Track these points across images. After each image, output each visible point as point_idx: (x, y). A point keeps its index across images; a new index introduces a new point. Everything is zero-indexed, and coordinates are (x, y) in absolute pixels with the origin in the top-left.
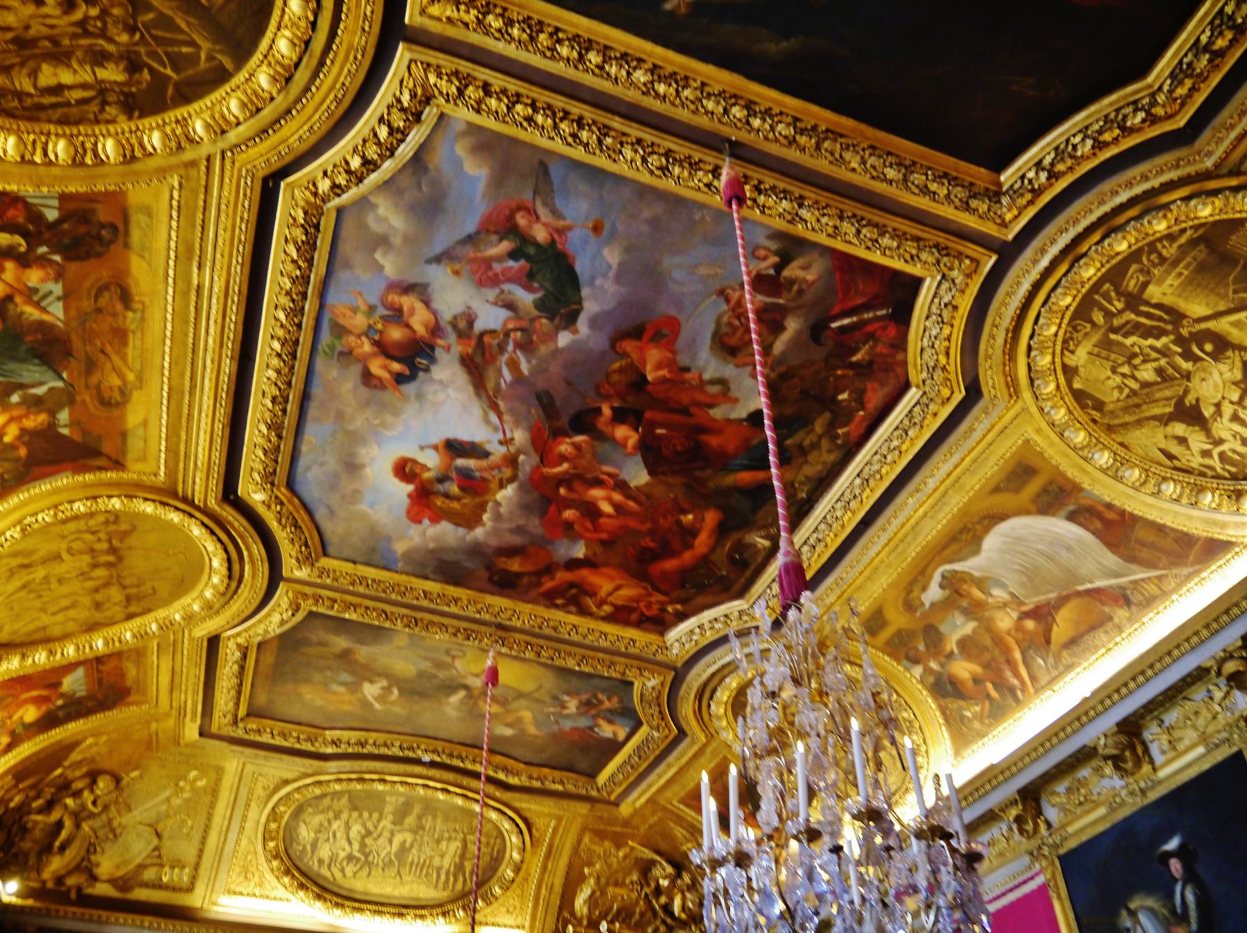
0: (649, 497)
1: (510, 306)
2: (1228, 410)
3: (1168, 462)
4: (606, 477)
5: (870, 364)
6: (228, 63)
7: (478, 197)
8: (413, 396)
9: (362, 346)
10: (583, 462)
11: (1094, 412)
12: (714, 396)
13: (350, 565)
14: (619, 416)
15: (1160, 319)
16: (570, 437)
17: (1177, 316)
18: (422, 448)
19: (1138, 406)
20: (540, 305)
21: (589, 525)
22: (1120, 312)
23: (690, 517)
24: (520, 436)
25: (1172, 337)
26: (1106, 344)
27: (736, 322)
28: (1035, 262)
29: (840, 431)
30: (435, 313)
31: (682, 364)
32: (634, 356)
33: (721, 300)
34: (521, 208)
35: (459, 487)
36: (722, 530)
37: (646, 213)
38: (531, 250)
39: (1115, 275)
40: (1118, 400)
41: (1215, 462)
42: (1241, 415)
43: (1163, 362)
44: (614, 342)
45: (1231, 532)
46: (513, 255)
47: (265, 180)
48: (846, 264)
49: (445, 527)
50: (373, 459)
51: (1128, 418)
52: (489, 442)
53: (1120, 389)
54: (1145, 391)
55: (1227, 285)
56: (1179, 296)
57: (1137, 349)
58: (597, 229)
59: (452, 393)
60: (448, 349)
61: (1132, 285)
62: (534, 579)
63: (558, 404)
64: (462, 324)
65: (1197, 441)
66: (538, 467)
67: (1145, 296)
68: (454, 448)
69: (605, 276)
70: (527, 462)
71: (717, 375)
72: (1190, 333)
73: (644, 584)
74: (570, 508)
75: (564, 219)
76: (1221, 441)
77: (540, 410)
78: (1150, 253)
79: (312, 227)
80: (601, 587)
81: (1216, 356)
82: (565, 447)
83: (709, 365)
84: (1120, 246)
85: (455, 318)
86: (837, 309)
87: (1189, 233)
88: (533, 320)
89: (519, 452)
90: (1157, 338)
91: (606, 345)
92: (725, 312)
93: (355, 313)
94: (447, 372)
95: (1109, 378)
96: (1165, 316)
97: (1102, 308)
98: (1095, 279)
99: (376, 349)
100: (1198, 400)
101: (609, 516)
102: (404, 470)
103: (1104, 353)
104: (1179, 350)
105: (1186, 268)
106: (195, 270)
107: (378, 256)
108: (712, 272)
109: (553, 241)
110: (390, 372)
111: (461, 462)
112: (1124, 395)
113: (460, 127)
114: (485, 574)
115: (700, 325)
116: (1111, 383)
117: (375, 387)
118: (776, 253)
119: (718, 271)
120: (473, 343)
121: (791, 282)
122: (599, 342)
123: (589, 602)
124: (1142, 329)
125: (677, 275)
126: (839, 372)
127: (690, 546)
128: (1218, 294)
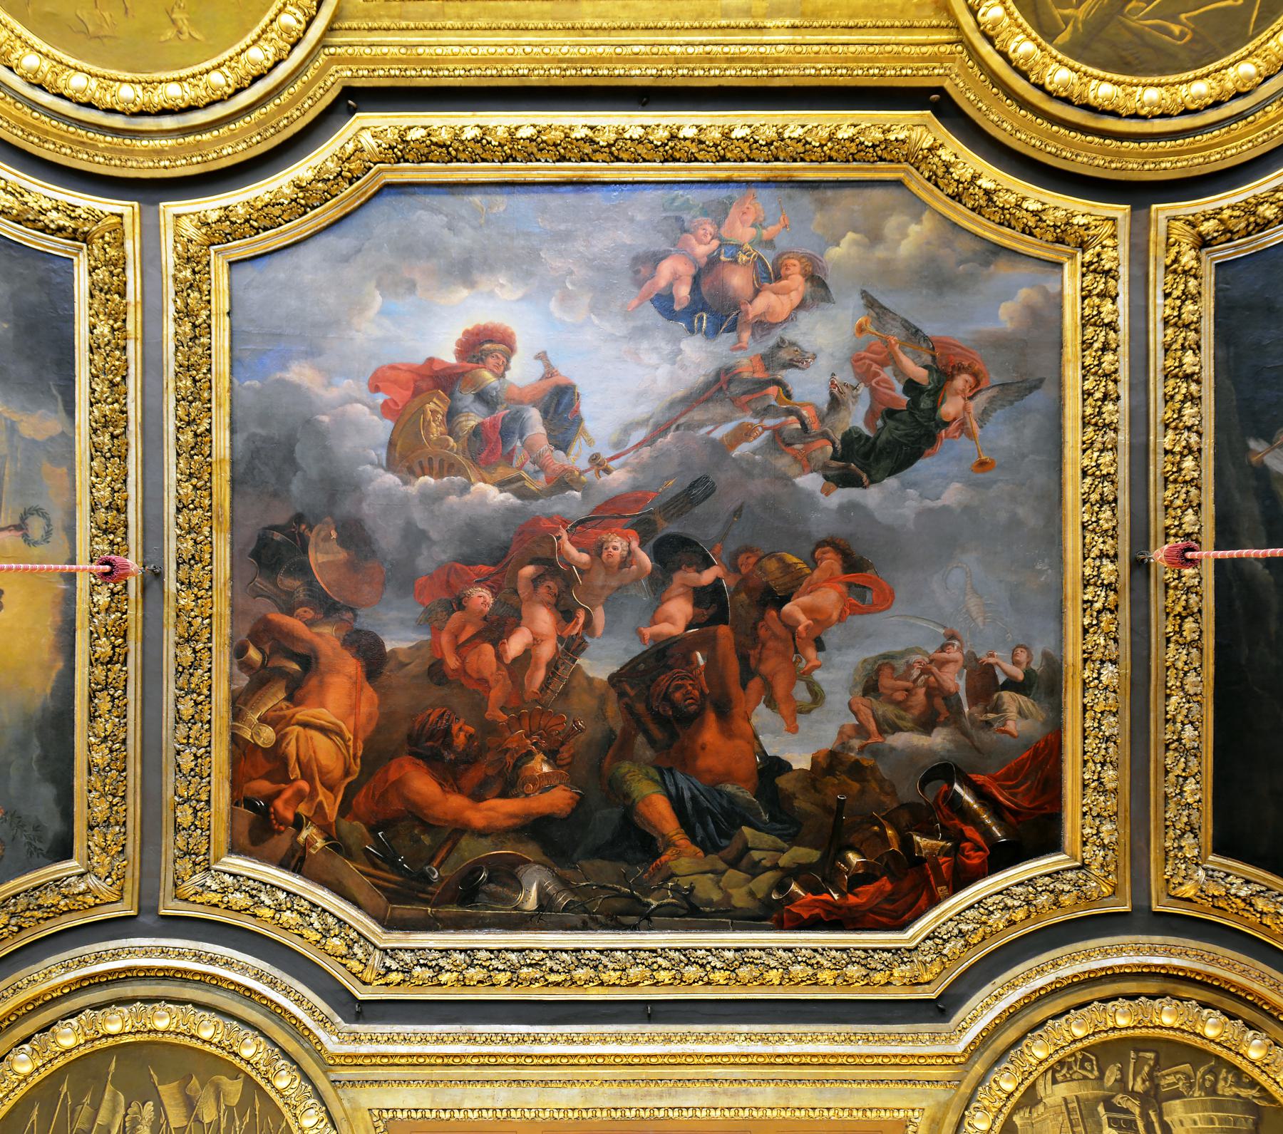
0: (565, 694)
1: (835, 403)
4: (581, 621)
5: (921, 860)
6: (1064, 37)
7: (972, 327)
8: (639, 323)
9: (700, 242)
10: (599, 579)
12: (790, 698)
13: (226, 307)
14: (700, 596)
16: (642, 545)
18: (542, 356)
20: (852, 439)
21: (469, 632)
22: (1133, 1094)
23: (546, 769)
24: (618, 479)
27: (916, 673)
28: (1153, 951)
29: (794, 887)
30: (791, 318)
31: (824, 638)
32: (816, 573)
33: (943, 640)
34: (975, 375)
35: (481, 425)
36: (537, 829)
37: (1021, 512)
38: (925, 403)
39: (1170, 1051)
44: (831, 543)
46: (911, 386)
47: (941, 90)
48: (1047, 755)
49: (383, 428)
50: (491, 295)
52: (590, 442)
58: (982, 464)
59: (664, 371)
60: (735, 349)
61: (1168, 1080)
62: (301, 595)
63: (697, 510)
64: (784, 355)
66: (565, 523)
67: (1164, 1105)
68: (560, 404)
69: (923, 496)
70: (572, 504)
71: (825, 688)
73: (356, 769)
74: (494, 595)
75: (981, 427)
77: (678, 490)
78: (1210, 1071)
79: (883, 151)
80: (322, 705)
82: (617, 545)
83: (837, 673)
84: (1212, 1027)
85: (793, 344)
86: (979, 778)
87: (1254, 1092)
88: (825, 435)
89: (585, 488)
91: (821, 533)
92: (926, 653)
93: (753, 226)
94: (698, 357)
97: (1123, 1071)
99: (704, 260)
101: (499, 657)
102: (484, 345)
105: (1222, 1121)
106: (788, 22)
107: (850, 235)
108: (974, 615)
109: (947, 424)
110: (670, 285)
111: (534, 416)
113: (1052, 288)
114: (281, 516)
115: (899, 632)
117: (637, 272)
118: (1029, 673)
119: (980, 620)
120: (760, 375)
121: (997, 708)
122: (821, 526)
123: (275, 698)
125: (956, 576)
126: (890, 832)
127: (477, 797)
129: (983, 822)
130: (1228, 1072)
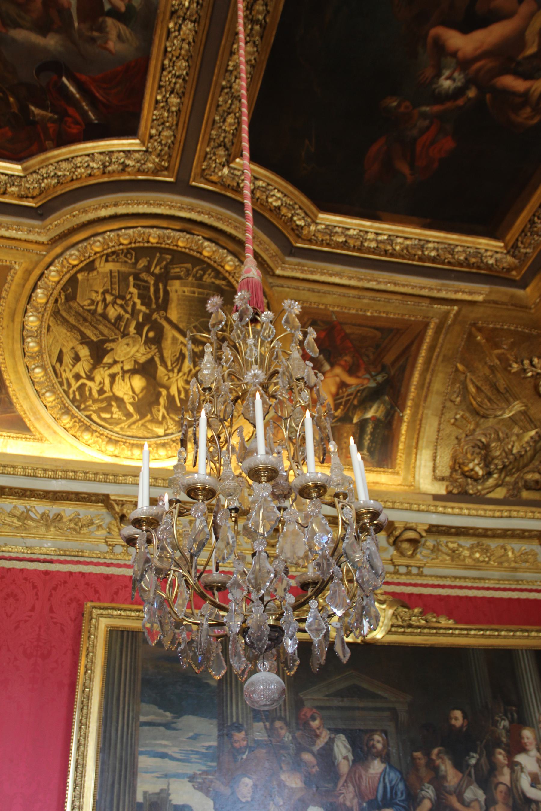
2: (116, 369)
3: (54, 360)
11: (63, 297)
15: (157, 298)
17: (164, 306)
19: (85, 320)
22: (153, 274)
25: (148, 311)
26: (123, 278)
40: (82, 307)
41: (75, 385)
42: (117, 378)
43: (127, 316)
45: (37, 425)
51: (72, 320)
53: (93, 302)
54: (100, 318)
55: (197, 320)
56: (178, 300)
57: (128, 297)
61: (176, 270)
65: (82, 367)
72: (156, 319)
76: (91, 378)
78: (202, 269)
81: (148, 342)
86: (83, 78)
87: (224, 283)
90: (142, 304)
95: (97, 292)
96: (160, 300)
98: (179, 249)
100: (112, 349)
103: (116, 280)
104: (141, 320)
105: (199, 293)
112: (88, 308)
116: (94, 296)
124: (145, 292)
126: (11, 99)
128: (189, 319)
129: (82, 107)
130: (212, 271)
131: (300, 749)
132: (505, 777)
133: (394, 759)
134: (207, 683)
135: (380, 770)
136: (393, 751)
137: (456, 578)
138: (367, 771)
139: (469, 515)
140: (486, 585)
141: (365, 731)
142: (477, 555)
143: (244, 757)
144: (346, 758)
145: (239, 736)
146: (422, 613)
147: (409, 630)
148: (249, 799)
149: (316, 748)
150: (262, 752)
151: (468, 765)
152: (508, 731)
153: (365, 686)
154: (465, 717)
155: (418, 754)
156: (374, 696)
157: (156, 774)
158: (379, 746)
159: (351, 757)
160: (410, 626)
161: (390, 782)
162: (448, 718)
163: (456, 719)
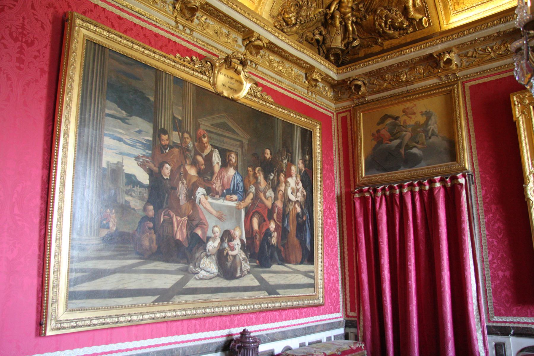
131: (197, 153)
132: (282, 188)
133: (240, 169)
134: (149, 98)
135: (233, 174)
136: (240, 163)
137: (270, 77)
138: (227, 173)
139: (288, 43)
140: (282, 86)
141: (229, 151)
142: (281, 68)
143: (167, 151)
144: (218, 163)
145: (164, 137)
146: (262, 91)
147: (254, 99)
148: (168, 178)
149: (205, 154)
150: (176, 150)
151: (269, 179)
152: (286, 165)
153: (230, 124)
154: (271, 154)
155: (250, 169)
156: (234, 132)
157: (114, 151)
158: (234, 160)
159: (220, 164)
160: (255, 96)
161: (237, 181)
162: (264, 153)
163: (267, 154)
